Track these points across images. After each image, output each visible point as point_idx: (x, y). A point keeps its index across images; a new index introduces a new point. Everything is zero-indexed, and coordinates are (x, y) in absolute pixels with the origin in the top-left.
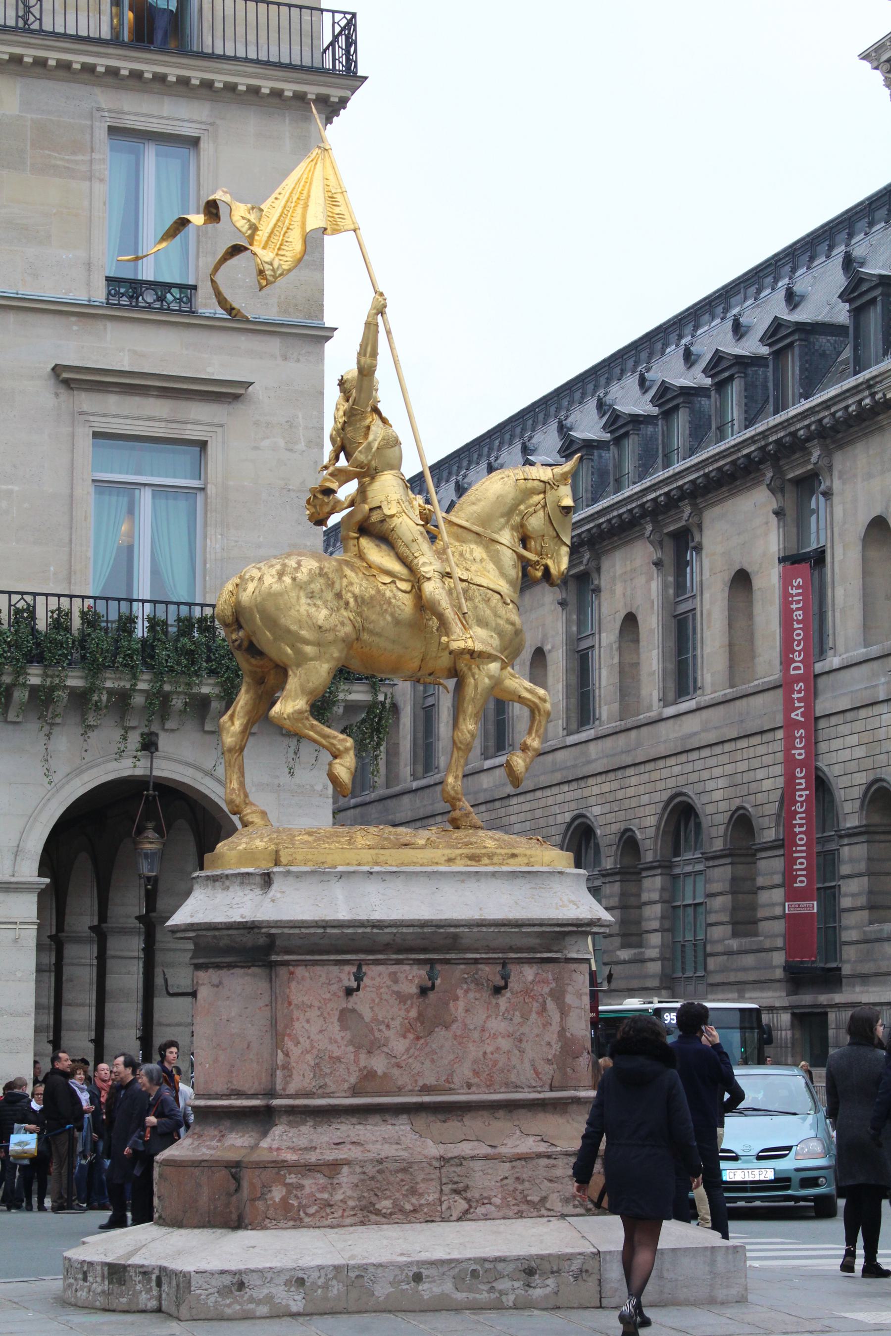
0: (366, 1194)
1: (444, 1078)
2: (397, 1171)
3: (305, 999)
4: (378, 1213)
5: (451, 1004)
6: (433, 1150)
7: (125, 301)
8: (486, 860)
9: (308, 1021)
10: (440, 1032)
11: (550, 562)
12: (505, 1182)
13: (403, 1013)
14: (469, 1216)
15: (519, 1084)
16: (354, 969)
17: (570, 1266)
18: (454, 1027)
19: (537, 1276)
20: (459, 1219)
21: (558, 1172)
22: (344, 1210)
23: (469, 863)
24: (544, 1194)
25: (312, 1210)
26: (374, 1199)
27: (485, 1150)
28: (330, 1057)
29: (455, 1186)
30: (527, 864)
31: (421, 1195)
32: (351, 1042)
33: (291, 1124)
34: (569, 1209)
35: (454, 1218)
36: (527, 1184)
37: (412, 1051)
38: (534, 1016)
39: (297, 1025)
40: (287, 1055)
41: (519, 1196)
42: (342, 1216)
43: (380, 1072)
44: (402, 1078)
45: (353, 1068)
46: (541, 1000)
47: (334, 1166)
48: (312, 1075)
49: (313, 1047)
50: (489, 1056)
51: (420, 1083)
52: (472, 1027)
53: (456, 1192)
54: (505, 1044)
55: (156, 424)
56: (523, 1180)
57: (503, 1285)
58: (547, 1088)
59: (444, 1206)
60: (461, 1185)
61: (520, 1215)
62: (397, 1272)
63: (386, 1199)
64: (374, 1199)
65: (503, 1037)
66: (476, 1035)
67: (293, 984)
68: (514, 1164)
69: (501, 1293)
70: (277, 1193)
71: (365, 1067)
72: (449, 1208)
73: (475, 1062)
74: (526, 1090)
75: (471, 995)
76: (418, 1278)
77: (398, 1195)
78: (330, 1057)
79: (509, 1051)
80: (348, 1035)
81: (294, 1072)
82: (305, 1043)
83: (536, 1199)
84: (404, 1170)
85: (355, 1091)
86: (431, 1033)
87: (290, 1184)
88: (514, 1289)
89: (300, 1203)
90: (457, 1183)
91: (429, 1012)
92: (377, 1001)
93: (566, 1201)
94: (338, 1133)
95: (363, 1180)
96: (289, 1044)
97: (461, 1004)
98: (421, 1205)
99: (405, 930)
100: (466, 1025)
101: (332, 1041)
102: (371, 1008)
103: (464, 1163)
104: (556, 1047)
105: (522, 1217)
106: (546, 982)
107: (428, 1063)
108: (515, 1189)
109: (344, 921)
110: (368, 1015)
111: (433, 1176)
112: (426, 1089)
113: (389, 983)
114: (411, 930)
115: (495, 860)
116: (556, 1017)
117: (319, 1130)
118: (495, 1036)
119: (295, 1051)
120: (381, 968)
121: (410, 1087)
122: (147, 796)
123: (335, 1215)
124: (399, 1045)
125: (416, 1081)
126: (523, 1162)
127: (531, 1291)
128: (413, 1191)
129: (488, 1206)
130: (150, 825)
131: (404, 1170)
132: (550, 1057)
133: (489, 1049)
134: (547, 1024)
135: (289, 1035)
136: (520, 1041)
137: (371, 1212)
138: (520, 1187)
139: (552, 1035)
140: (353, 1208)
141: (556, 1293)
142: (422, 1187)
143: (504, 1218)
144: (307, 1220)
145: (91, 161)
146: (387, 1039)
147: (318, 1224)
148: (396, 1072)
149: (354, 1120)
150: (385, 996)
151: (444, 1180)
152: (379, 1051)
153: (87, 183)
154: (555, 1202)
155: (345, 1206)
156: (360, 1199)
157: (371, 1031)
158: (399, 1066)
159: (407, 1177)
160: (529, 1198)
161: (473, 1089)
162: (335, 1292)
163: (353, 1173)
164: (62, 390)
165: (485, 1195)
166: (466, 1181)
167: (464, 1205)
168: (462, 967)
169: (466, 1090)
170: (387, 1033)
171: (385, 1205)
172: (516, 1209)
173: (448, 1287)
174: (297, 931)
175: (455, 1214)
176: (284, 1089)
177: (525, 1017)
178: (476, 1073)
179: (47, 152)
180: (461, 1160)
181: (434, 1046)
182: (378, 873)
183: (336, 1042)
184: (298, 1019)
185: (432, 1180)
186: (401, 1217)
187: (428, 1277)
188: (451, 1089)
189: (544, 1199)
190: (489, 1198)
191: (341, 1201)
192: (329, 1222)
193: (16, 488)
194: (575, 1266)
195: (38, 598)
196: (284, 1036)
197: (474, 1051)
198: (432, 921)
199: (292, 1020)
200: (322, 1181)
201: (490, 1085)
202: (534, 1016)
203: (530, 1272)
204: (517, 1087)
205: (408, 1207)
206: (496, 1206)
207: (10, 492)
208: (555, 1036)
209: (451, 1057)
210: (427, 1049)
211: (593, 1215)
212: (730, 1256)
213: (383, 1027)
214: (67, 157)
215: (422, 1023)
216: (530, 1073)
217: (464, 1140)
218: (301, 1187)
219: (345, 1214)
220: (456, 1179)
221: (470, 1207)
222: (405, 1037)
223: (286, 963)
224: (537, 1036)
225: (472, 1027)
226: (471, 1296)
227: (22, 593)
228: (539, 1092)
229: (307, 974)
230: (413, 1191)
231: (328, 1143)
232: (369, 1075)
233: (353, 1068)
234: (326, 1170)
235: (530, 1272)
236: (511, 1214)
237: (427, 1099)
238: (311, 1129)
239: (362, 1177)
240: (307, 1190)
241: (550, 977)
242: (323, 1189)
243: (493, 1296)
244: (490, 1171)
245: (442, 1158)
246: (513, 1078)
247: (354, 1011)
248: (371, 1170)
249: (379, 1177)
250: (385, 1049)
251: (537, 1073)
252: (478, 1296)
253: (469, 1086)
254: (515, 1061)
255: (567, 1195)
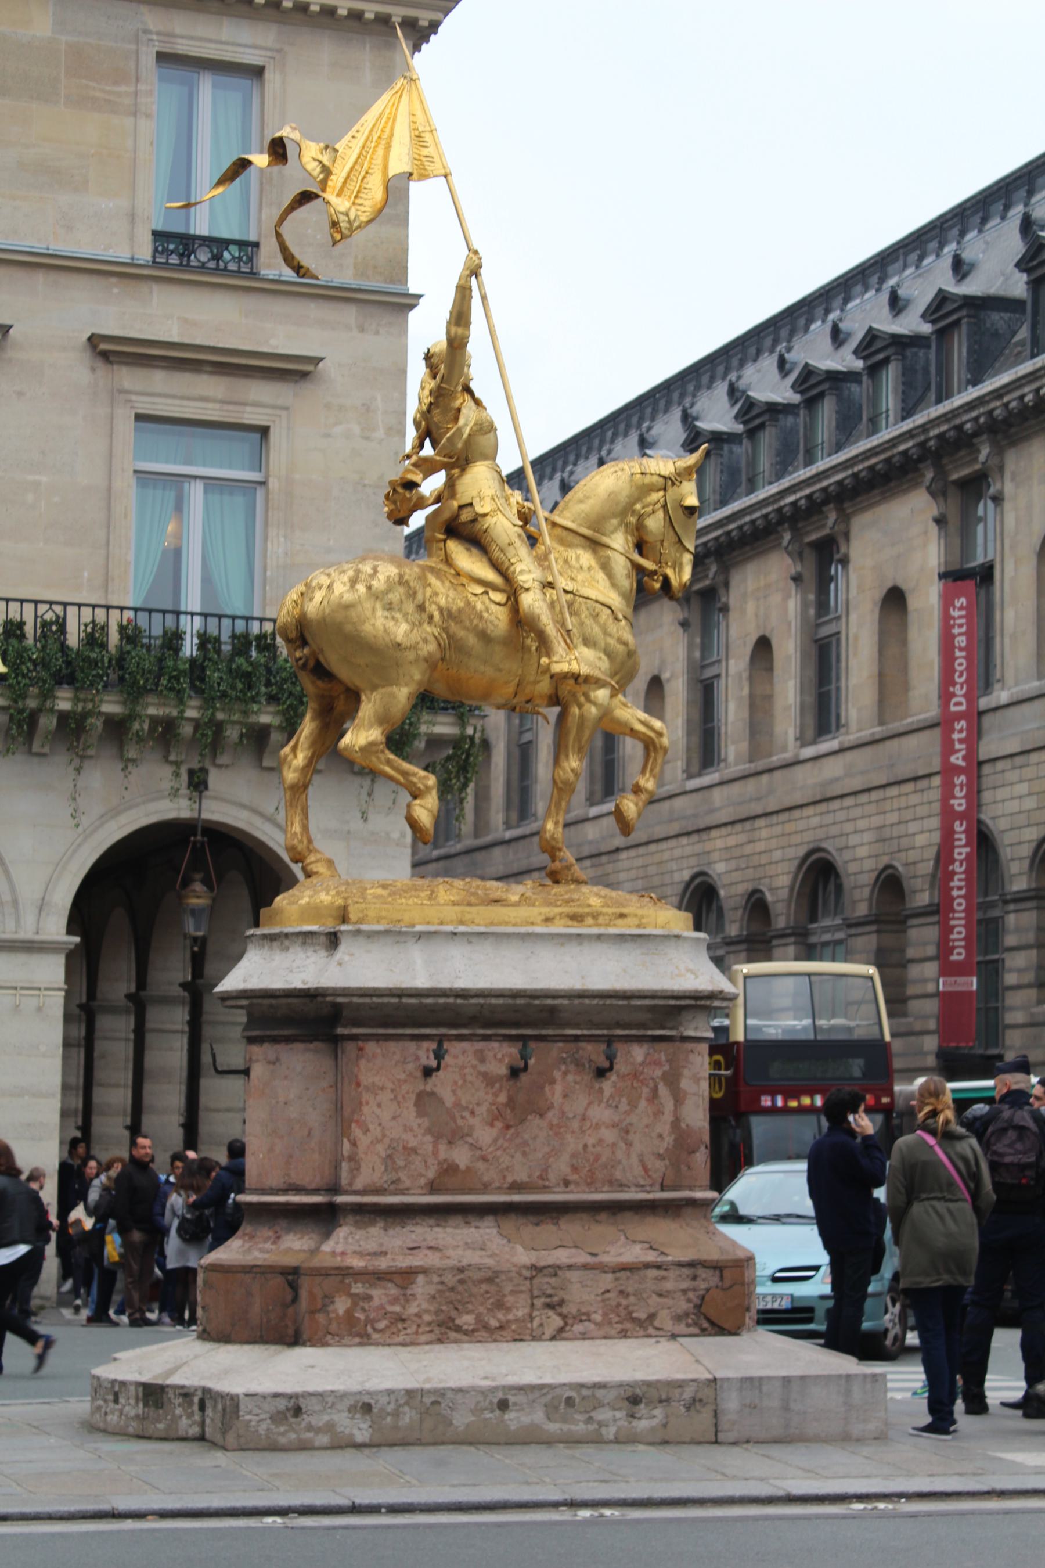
0: (444, 1308)
1: (537, 1173)
2: (481, 1281)
3: (376, 1079)
4: (458, 1329)
5: (547, 1089)
6: (523, 1257)
7: (174, 260)
8: (589, 921)
9: (379, 1105)
10: (534, 1122)
11: (669, 572)
12: (607, 1295)
13: (490, 1098)
14: (564, 1335)
15: (625, 1182)
16: (434, 1046)
17: (681, 1394)
18: (550, 1114)
19: (642, 1406)
20: (553, 1338)
21: (669, 1285)
22: (419, 1326)
23: (570, 923)
24: (652, 1310)
25: (381, 1325)
26: (453, 1314)
27: (583, 1258)
28: (405, 1148)
29: (548, 1300)
30: (638, 926)
31: (508, 1310)
32: (429, 1131)
33: (358, 1225)
34: (682, 1328)
35: (547, 1335)
36: (632, 1299)
37: (500, 1142)
38: (643, 1104)
39: (366, 1109)
40: (354, 1144)
41: (623, 1313)
42: (417, 1333)
43: (462, 1167)
44: (489, 1174)
45: (431, 1161)
46: (652, 1084)
47: (406, 1276)
48: (383, 1168)
49: (384, 1136)
50: (590, 1149)
51: (510, 1179)
52: (571, 1115)
53: (550, 1306)
54: (609, 1135)
55: (210, 405)
56: (628, 1295)
57: (603, 1415)
58: (657, 1187)
59: (536, 1323)
60: (556, 1299)
61: (624, 1334)
62: (480, 1398)
63: (468, 1313)
64: (453, 1314)
65: (607, 1127)
66: (575, 1125)
67: (363, 1063)
68: (618, 1275)
69: (601, 1424)
70: (341, 1305)
71: (445, 1160)
72: (541, 1325)
73: (574, 1155)
74: (633, 1189)
75: (570, 1078)
76: (503, 1405)
77: (481, 1309)
78: (405, 1148)
79: (614, 1145)
80: (426, 1122)
81: (363, 1164)
82: (375, 1130)
83: (642, 1315)
84: (490, 1280)
85: (433, 1188)
86: (522, 1121)
87: (357, 1295)
88: (615, 1420)
89: (367, 1317)
90: (550, 1296)
91: (520, 1098)
92: (460, 1082)
93: (678, 1318)
94: (413, 1236)
95: (440, 1291)
96: (357, 1132)
97: (558, 1088)
98: (508, 1321)
99: (494, 1001)
100: (563, 1113)
101: (407, 1129)
102: (454, 1092)
103: (560, 1273)
104: (669, 1140)
105: (625, 1337)
106: (657, 1063)
107: (518, 1156)
108: (619, 1305)
109: (423, 989)
110: (449, 1100)
111: (523, 1288)
112: (516, 1187)
113: (475, 1062)
114: (501, 1001)
115: (601, 920)
116: (669, 1105)
117: (391, 1232)
118: (597, 1126)
119: (364, 1141)
120: (465, 1045)
121: (497, 1184)
122: (195, 843)
123: (409, 1331)
124: (485, 1135)
125: (504, 1177)
126: (628, 1273)
127: (635, 1423)
128: (500, 1305)
129: (586, 1323)
130: (198, 876)
131: (490, 1280)
132: (661, 1151)
133: (591, 1141)
134: (658, 1113)
135: (357, 1122)
136: (627, 1132)
137: (450, 1328)
138: (624, 1302)
139: (664, 1126)
140: (429, 1324)
141: (665, 1426)
142: (510, 1300)
143: (605, 1338)
144: (375, 1336)
145: (136, 94)
146: (471, 1128)
147: (388, 1341)
148: (481, 1166)
149: (432, 1221)
150: (469, 1078)
151: (536, 1293)
152: (461, 1142)
153: (132, 119)
154: (664, 1320)
155: (419, 1321)
156: (438, 1312)
157: (453, 1118)
158: (484, 1159)
159: (493, 1289)
160: (634, 1315)
161: (572, 1187)
162: (407, 1420)
163: (430, 1282)
164: (100, 364)
165: (584, 1310)
166: (562, 1294)
167: (558, 1322)
168: (560, 1044)
169: (562, 1189)
170: (472, 1121)
171: (467, 1320)
172: (619, 1327)
173: (538, 1416)
174: (367, 1000)
175: (549, 1332)
176: (350, 1184)
177: (633, 1105)
178: (575, 1169)
179: (84, 82)
180: (555, 1270)
181: (526, 1136)
182: (463, 934)
183: (411, 1130)
184: (367, 1103)
185: (521, 1292)
186: (484, 1334)
187: (515, 1404)
188: (545, 1187)
189: (652, 1317)
190: (588, 1314)
191: (416, 1315)
192: (401, 1339)
193: (44, 479)
194: (688, 1394)
195: (69, 608)
196: (351, 1121)
197: (572, 1143)
198: (525, 990)
199: (361, 1103)
200: (394, 1291)
201: (591, 1183)
202: (643, 1104)
203: (635, 1400)
204: (622, 1186)
205: (494, 1323)
206: (596, 1324)
208: (668, 1127)
209: (547, 1149)
210: (518, 1141)
211: (710, 1335)
212: (868, 1386)
213: (466, 1114)
214: (108, 88)
215: (513, 1109)
216: (638, 1170)
217: (558, 1247)
218: (369, 1298)
219: (420, 1330)
220: (549, 1291)
221: (566, 1324)
222: (492, 1125)
223: (354, 1038)
224: (647, 1126)
225: (571, 1115)
226: (566, 1427)
227: (51, 603)
228: (649, 1192)
229: (379, 1051)
230: (500, 1305)
231: (401, 1247)
232: (449, 1169)
233: (431, 1161)
234: (397, 1279)
235: (635, 1400)
236: (613, 1332)
237: (516, 1198)
238: (382, 1232)
239: (440, 1287)
240: (376, 1302)
241: (663, 1058)
242: (395, 1301)
243: (591, 1427)
244: (589, 1283)
245: (533, 1267)
246: (618, 1175)
247: (432, 1094)
248: (450, 1279)
249: (460, 1288)
250: (470, 1140)
251: (646, 1170)
252: (573, 1427)
253: (566, 1183)
254: (620, 1154)
255: (679, 1311)
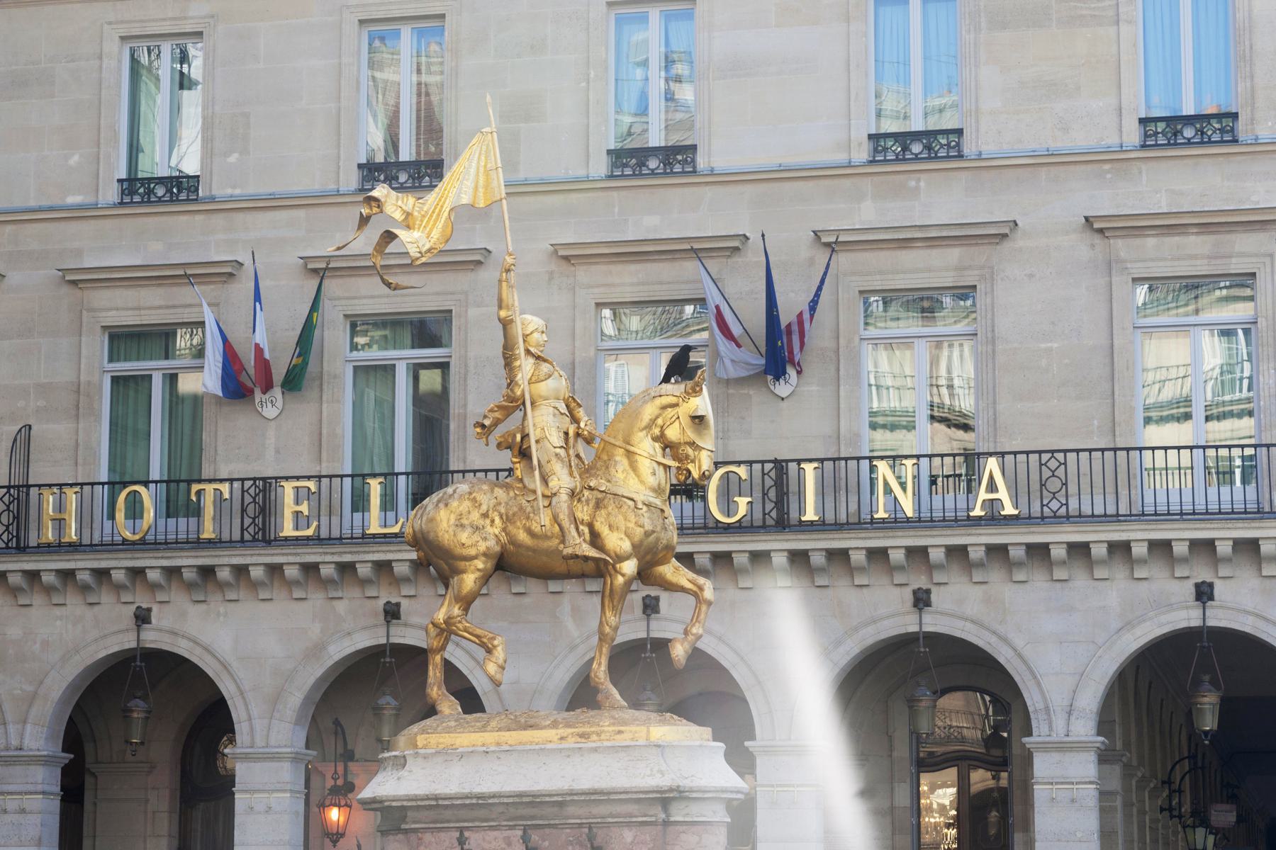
7: (1162, 140)
8: (594, 737)
16: (457, 834)
30: (632, 739)
55: (1199, 262)
115: (603, 737)
120: (496, 833)
130: (1207, 678)
153: (1112, 30)
182: (493, 752)
193: (1055, 345)
207: (1051, 349)
223: (415, 831)
227: (1053, 452)
241: (648, 838)
